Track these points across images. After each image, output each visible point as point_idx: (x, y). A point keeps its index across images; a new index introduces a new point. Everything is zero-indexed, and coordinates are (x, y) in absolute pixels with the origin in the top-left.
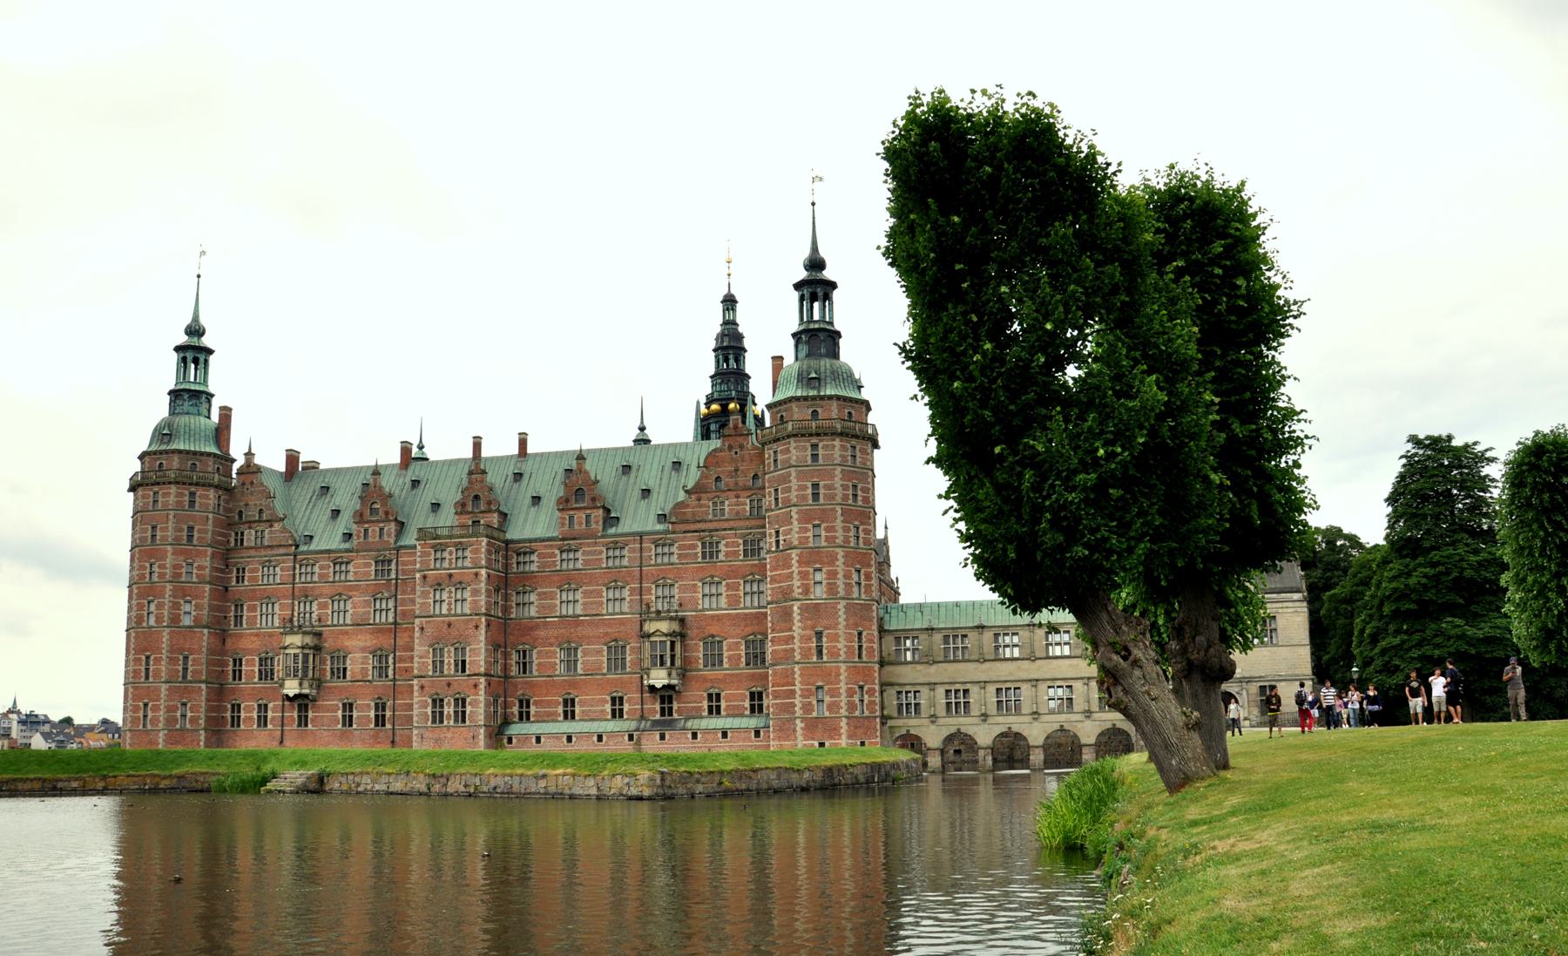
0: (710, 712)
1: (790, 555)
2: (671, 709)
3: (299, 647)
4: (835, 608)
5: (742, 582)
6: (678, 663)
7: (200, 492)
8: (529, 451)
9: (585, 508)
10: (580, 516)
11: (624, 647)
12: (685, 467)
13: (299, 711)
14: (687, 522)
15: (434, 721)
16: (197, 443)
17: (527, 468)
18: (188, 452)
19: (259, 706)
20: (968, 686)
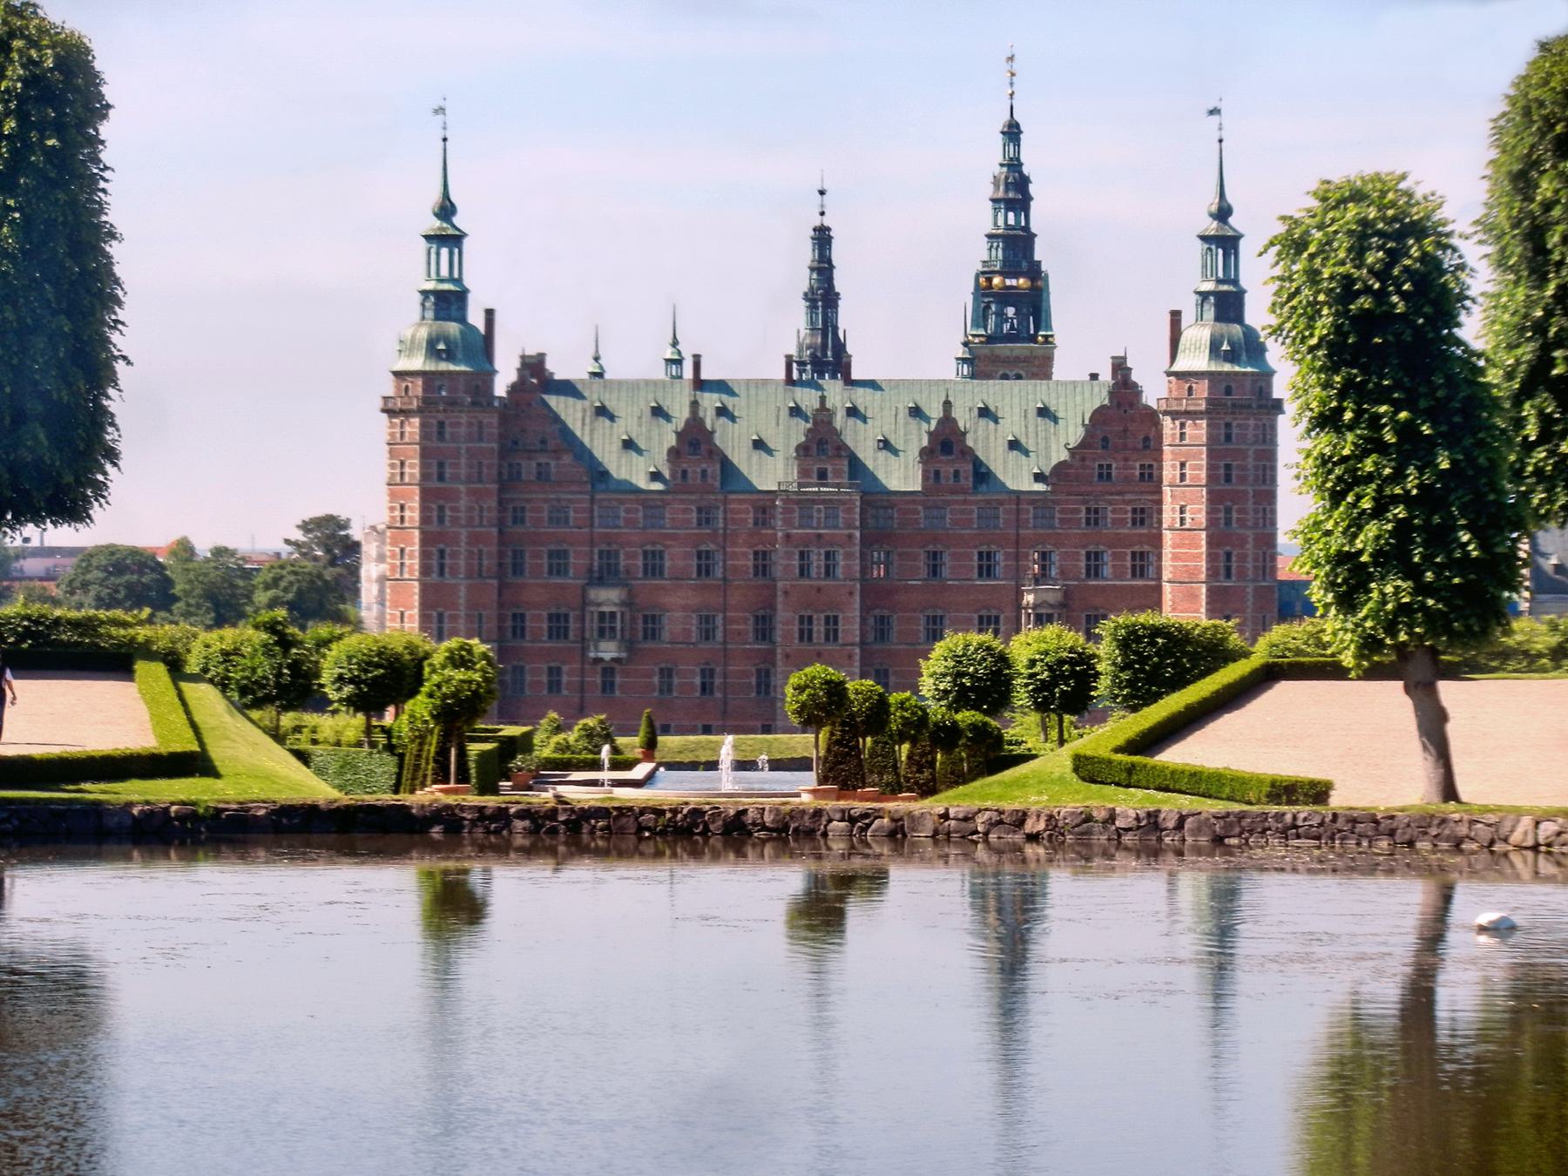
3: (616, 604)
10: (947, 470)
19: (550, 670)
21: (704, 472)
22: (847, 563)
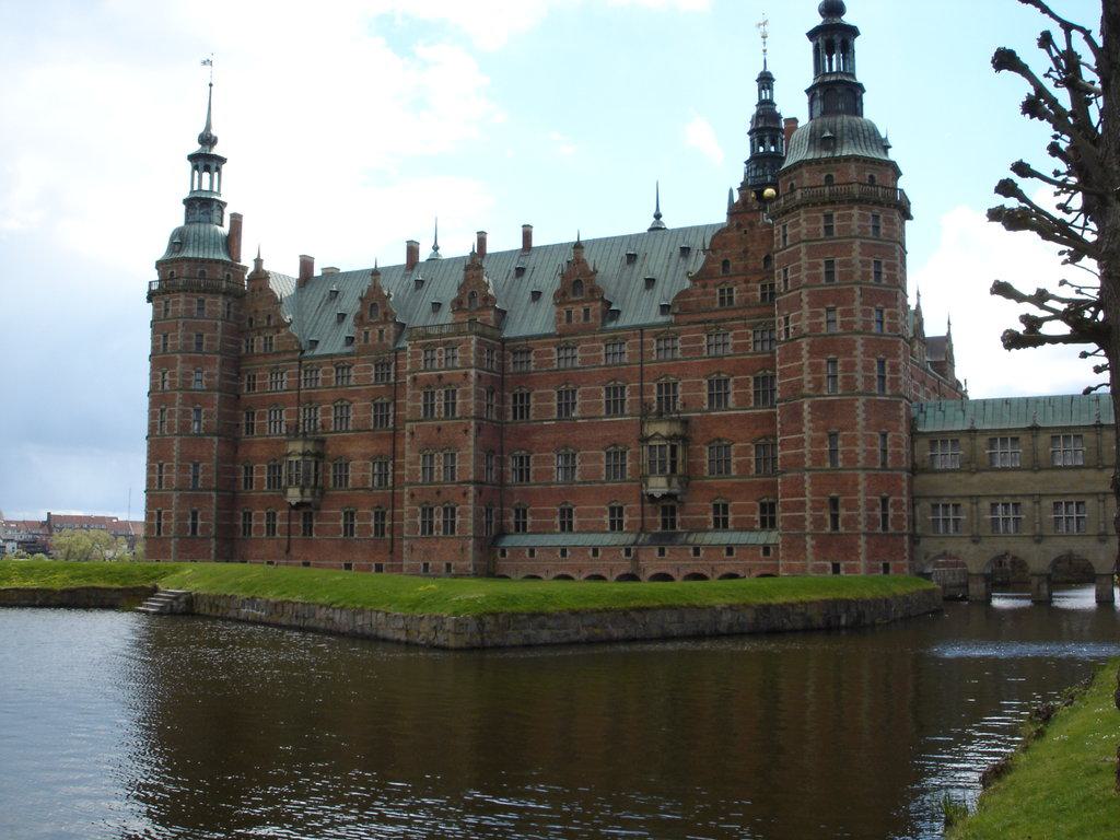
0: (717, 525)
1: (799, 344)
2: (673, 521)
3: (299, 454)
4: (852, 405)
5: (751, 378)
6: (680, 469)
7: (208, 299)
8: (535, 243)
9: (583, 301)
10: (578, 310)
11: (623, 453)
12: (694, 253)
13: (305, 519)
14: (692, 312)
15: (423, 532)
16: (206, 250)
17: (529, 262)
18: (196, 260)
20: (1019, 500)
21: (381, 332)
22: (467, 402)
